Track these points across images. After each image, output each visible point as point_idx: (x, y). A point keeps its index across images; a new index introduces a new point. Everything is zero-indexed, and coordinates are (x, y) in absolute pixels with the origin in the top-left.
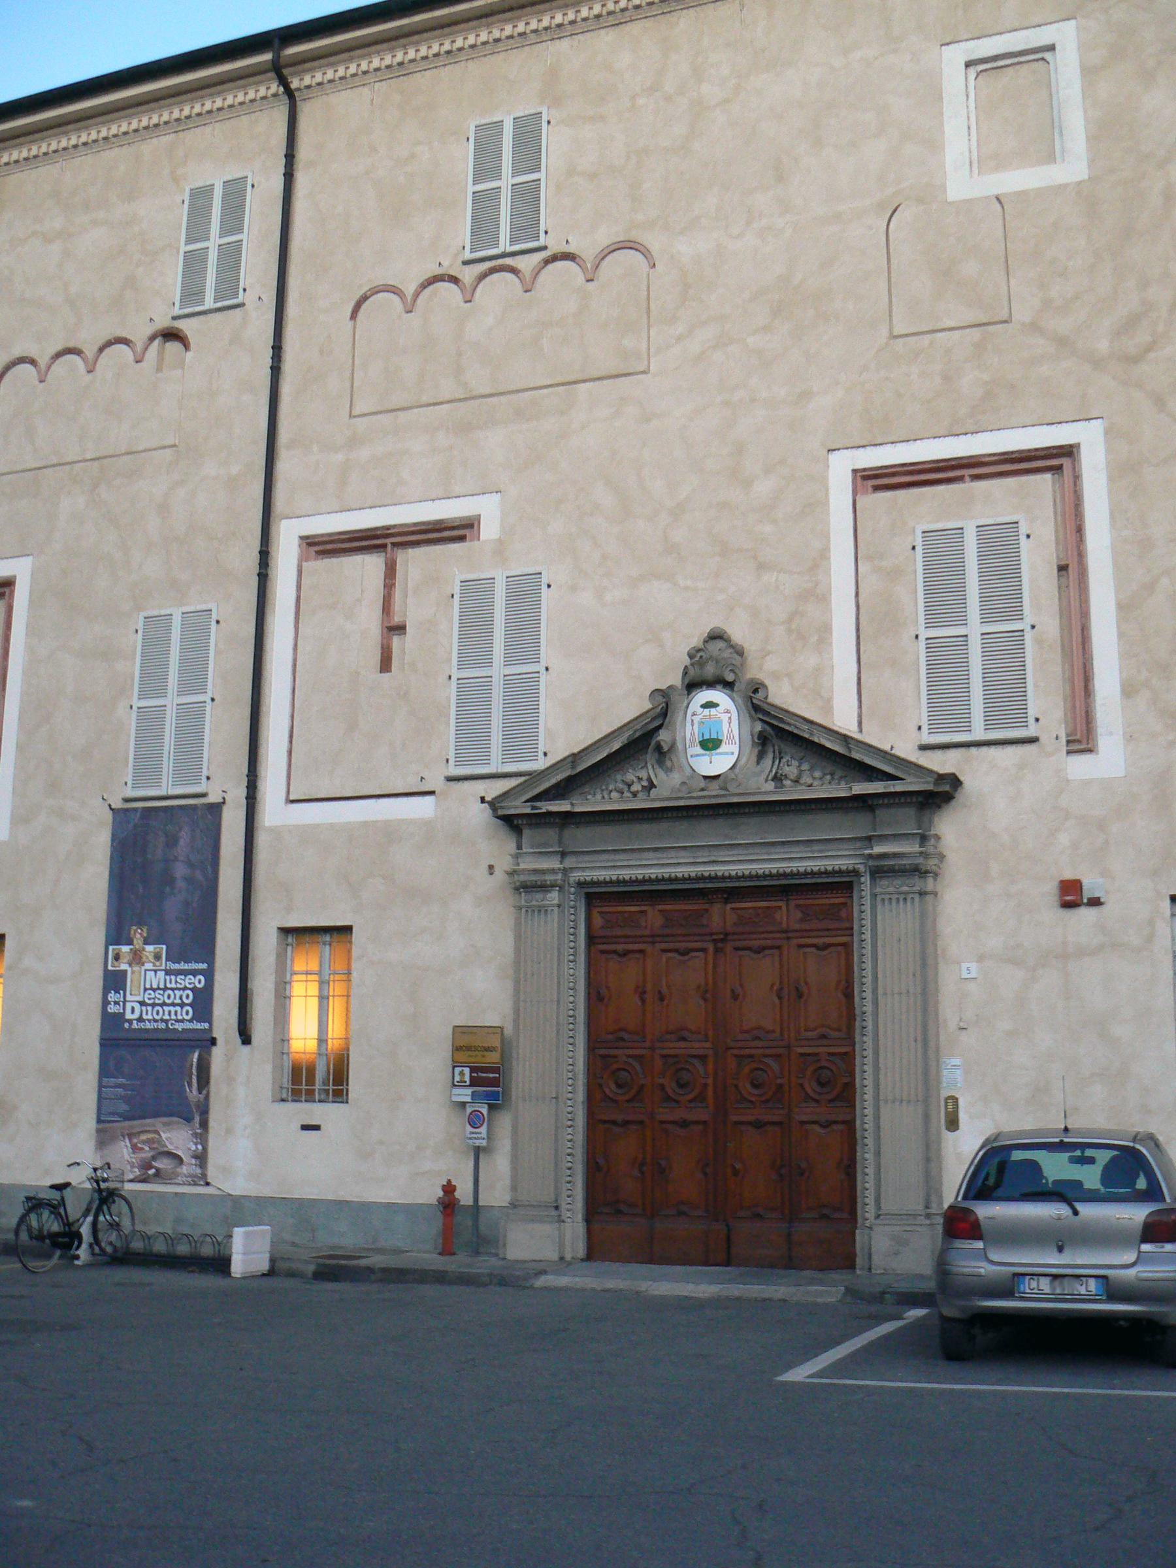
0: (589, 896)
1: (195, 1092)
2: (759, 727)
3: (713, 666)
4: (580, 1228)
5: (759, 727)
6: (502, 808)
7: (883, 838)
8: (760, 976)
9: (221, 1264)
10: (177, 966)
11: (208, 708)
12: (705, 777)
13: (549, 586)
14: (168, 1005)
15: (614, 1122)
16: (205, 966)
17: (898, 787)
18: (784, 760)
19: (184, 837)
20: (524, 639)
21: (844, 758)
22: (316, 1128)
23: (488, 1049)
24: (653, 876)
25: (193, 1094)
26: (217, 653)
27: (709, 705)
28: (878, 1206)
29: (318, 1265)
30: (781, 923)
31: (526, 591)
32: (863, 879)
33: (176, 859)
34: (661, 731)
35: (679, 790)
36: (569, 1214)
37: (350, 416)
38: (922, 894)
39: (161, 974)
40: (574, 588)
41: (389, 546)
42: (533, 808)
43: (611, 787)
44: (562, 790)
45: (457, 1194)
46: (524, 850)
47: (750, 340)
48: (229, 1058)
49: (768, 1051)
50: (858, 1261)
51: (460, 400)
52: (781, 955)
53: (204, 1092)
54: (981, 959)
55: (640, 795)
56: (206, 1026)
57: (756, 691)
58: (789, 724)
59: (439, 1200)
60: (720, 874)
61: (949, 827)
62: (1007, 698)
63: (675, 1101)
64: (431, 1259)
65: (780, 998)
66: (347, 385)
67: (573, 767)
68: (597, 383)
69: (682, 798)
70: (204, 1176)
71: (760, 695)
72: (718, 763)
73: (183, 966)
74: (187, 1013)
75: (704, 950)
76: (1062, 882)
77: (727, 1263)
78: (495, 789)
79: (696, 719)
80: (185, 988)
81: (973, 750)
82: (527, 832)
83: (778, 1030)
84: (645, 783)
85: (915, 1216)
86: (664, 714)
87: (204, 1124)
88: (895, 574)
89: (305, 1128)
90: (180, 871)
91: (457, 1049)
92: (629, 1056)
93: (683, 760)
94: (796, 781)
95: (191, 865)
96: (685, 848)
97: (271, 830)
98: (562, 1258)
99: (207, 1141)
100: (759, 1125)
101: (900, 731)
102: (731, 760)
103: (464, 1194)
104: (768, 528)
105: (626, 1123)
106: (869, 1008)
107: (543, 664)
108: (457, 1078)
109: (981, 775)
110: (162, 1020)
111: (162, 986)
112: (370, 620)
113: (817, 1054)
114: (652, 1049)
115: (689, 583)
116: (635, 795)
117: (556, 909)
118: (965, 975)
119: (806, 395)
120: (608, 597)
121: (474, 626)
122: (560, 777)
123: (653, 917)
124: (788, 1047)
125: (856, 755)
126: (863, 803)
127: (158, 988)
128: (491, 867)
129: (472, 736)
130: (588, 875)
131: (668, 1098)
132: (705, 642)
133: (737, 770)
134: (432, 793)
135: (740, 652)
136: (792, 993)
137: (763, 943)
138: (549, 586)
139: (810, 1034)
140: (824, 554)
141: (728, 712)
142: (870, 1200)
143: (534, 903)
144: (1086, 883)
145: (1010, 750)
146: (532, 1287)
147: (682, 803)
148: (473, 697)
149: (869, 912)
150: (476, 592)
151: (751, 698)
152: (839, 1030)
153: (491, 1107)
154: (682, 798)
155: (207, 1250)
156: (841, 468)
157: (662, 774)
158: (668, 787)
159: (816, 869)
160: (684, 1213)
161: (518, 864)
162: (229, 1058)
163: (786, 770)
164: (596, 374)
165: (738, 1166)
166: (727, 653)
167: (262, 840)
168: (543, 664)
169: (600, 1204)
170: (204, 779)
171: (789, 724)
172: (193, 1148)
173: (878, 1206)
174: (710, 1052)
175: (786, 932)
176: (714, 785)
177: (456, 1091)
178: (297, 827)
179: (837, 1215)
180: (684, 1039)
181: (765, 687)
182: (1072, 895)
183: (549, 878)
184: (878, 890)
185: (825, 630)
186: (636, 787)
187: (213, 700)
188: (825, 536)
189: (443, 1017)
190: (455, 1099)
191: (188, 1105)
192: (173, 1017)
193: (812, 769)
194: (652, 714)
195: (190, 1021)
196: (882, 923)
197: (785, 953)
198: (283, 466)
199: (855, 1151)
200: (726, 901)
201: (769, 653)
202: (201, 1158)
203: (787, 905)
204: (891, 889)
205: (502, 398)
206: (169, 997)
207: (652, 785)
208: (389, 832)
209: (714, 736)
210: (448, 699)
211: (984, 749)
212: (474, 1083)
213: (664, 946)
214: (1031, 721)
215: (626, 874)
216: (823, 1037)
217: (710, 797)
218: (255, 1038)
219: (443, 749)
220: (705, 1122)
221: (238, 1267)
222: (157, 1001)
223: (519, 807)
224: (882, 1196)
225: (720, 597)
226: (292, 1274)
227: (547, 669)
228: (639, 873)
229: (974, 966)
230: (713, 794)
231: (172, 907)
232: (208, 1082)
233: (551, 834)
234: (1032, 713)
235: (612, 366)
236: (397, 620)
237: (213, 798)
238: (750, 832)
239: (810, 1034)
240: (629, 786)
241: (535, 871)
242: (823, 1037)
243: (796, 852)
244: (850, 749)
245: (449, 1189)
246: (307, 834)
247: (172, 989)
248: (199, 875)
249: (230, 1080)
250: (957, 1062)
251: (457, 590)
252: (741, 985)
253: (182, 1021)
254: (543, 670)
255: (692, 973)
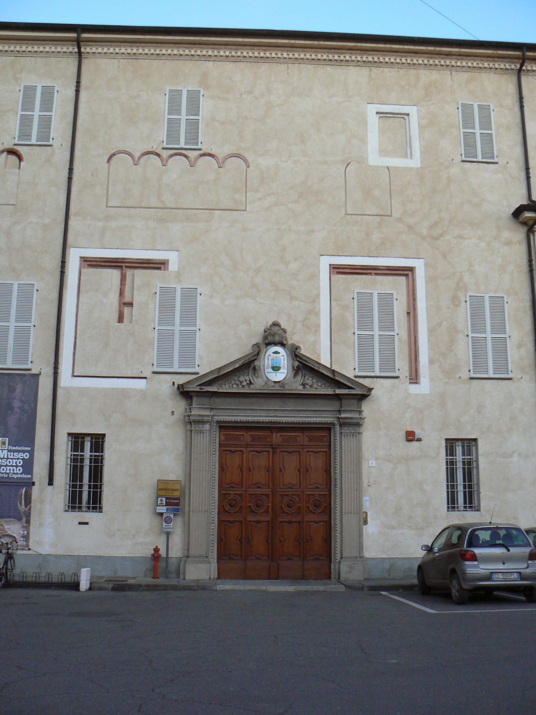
0: (220, 427)
1: (23, 506)
2: (297, 363)
3: (273, 337)
4: (216, 565)
5: (297, 363)
6: (186, 388)
7: (345, 411)
8: (291, 463)
9: (76, 586)
10: (14, 448)
11: (32, 331)
12: (274, 382)
13: (201, 294)
14: (9, 466)
15: (229, 521)
16: (29, 449)
17: (354, 392)
18: (306, 377)
19: (19, 389)
20: (190, 316)
21: (332, 379)
22: (87, 523)
23: (174, 490)
24: (250, 421)
25: (22, 508)
26: (37, 304)
27: (276, 353)
28: (342, 554)
29: (114, 584)
30: (300, 442)
31: (190, 296)
32: (336, 427)
33: (14, 398)
34: (256, 361)
35: (264, 386)
36: (212, 560)
37: (107, 206)
38: (359, 433)
39: (5, 452)
40: (211, 297)
41: (124, 267)
42: (201, 389)
43: (233, 382)
44: (210, 383)
45: (160, 552)
46: (193, 406)
47: (289, 205)
48: (41, 491)
49: (293, 493)
50: (332, 576)
51: (160, 208)
52: (300, 456)
53: (28, 507)
54: (377, 459)
55: (246, 387)
56: (30, 476)
57: (297, 349)
58: (310, 363)
59: (153, 555)
60: (278, 421)
61: (366, 407)
62: (388, 361)
63: (255, 513)
64: (149, 580)
65: (299, 472)
66: (105, 192)
67: (218, 373)
68: (224, 211)
69: (265, 390)
70: (27, 545)
71: (298, 351)
72: (279, 376)
73: (17, 448)
74: (19, 470)
75: (268, 452)
76: (407, 432)
77: (277, 578)
78: (181, 380)
79: (270, 358)
80: (18, 459)
81: (375, 379)
82: (194, 399)
83: (298, 484)
84: (248, 382)
85: (356, 558)
86: (258, 354)
87: (28, 522)
88: (346, 307)
89: (80, 523)
90: (16, 404)
91: (159, 489)
92: (235, 494)
93: (263, 374)
94: (311, 386)
95: (23, 402)
96: (264, 410)
97: (64, 388)
98: (210, 578)
99: (29, 530)
100: (290, 522)
101: (348, 369)
102: (285, 375)
103: (163, 552)
104: (295, 283)
105: (234, 522)
106: (338, 477)
107: (198, 327)
108: (159, 502)
109: (380, 389)
110: (6, 473)
111: (6, 457)
112: (114, 298)
113: (314, 495)
114: (246, 491)
115: (262, 301)
116: (243, 386)
117: (208, 432)
118: (370, 465)
119: (312, 232)
120: (227, 302)
121: (166, 307)
122: (213, 377)
123: (247, 437)
124: (303, 492)
125: (337, 378)
126: (338, 397)
127: (4, 458)
128: (173, 412)
129: (165, 354)
130: (222, 418)
131: (252, 511)
132: (271, 326)
133: (286, 380)
134: (146, 378)
135: (285, 331)
136: (303, 470)
137: (293, 450)
138: (201, 294)
139: (311, 487)
140: (318, 296)
141: (283, 356)
142: (338, 552)
143: (198, 429)
144: (417, 432)
145: (389, 380)
146: (216, 590)
147: (265, 392)
148: (165, 339)
149: (338, 440)
150: (167, 294)
151: (295, 351)
152: (323, 485)
153: (175, 515)
154: (265, 390)
155: (68, 579)
156: (325, 263)
157: (255, 379)
158: (258, 385)
159: (318, 422)
160: (259, 559)
161: (191, 412)
162: (41, 491)
163: (307, 381)
164: (222, 208)
165: (282, 539)
166: (280, 332)
167: (60, 392)
168: (198, 327)
169: (224, 554)
170: (30, 362)
171: (310, 363)
172: (22, 533)
173: (342, 554)
174: (270, 493)
175: (303, 446)
176: (277, 385)
177: (158, 508)
178: (78, 388)
179: (321, 558)
180: (259, 487)
181: (300, 348)
182: (410, 436)
183: (206, 419)
184: (343, 431)
185: (318, 326)
186: (244, 383)
187: (34, 326)
188: (318, 289)
189: (150, 477)
190: (158, 511)
191: (20, 513)
192: (12, 472)
193: (317, 382)
194: (253, 354)
195: (21, 474)
196: (342, 443)
197: (302, 454)
198: (72, 223)
199: (331, 533)
200: (278, 432)
201: (295, 333)
202: (26, 538)
203: (303, 435)
204: (348, 431)
205: (181, 211)
206: (10, 462)
207: (251, 383)
208: (124, 393)
209: (278, 365)
210: (154, 338)
211: (379, 379)
212: (167, 504)
213: (251, 449)
214: (397, 370)
215: (238, 419)
216: (317, 488)
217: (275, 390)
218: (55, 482)
219: (151, 359)
220: (268, 522)
221: (84, 585)
222: (3, 464)
223: (194, 388)
224: (344, 549)
225: (275, 308)
226: (100, 589)
227: (199, 330)
228: (244, 419)
229: (374, 462)
230: (277, 389)
231: (12, 420)
232: (30, 502)
233: (206, 400)
234: (397, 367)
235: (231, 205)
236: (127, 299)
237: (33, 372)
238: (290, 405)
239: (311, 487)
240: (241, 383)
241: (200, 415)
242: (317, 488)
243: (309, 414)
244: (334, 376)
245: (156, 550)
246: (83, 392)
247: (12, 459)
248: (26, 407)
249: (42, 502)
250: (367, 498)
251: (158, 291)
252: (284, 466)
253: (17, 474)
254: (198, 330)
255: (262, 461)
